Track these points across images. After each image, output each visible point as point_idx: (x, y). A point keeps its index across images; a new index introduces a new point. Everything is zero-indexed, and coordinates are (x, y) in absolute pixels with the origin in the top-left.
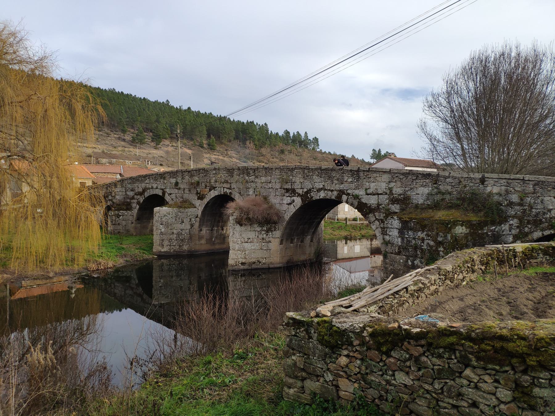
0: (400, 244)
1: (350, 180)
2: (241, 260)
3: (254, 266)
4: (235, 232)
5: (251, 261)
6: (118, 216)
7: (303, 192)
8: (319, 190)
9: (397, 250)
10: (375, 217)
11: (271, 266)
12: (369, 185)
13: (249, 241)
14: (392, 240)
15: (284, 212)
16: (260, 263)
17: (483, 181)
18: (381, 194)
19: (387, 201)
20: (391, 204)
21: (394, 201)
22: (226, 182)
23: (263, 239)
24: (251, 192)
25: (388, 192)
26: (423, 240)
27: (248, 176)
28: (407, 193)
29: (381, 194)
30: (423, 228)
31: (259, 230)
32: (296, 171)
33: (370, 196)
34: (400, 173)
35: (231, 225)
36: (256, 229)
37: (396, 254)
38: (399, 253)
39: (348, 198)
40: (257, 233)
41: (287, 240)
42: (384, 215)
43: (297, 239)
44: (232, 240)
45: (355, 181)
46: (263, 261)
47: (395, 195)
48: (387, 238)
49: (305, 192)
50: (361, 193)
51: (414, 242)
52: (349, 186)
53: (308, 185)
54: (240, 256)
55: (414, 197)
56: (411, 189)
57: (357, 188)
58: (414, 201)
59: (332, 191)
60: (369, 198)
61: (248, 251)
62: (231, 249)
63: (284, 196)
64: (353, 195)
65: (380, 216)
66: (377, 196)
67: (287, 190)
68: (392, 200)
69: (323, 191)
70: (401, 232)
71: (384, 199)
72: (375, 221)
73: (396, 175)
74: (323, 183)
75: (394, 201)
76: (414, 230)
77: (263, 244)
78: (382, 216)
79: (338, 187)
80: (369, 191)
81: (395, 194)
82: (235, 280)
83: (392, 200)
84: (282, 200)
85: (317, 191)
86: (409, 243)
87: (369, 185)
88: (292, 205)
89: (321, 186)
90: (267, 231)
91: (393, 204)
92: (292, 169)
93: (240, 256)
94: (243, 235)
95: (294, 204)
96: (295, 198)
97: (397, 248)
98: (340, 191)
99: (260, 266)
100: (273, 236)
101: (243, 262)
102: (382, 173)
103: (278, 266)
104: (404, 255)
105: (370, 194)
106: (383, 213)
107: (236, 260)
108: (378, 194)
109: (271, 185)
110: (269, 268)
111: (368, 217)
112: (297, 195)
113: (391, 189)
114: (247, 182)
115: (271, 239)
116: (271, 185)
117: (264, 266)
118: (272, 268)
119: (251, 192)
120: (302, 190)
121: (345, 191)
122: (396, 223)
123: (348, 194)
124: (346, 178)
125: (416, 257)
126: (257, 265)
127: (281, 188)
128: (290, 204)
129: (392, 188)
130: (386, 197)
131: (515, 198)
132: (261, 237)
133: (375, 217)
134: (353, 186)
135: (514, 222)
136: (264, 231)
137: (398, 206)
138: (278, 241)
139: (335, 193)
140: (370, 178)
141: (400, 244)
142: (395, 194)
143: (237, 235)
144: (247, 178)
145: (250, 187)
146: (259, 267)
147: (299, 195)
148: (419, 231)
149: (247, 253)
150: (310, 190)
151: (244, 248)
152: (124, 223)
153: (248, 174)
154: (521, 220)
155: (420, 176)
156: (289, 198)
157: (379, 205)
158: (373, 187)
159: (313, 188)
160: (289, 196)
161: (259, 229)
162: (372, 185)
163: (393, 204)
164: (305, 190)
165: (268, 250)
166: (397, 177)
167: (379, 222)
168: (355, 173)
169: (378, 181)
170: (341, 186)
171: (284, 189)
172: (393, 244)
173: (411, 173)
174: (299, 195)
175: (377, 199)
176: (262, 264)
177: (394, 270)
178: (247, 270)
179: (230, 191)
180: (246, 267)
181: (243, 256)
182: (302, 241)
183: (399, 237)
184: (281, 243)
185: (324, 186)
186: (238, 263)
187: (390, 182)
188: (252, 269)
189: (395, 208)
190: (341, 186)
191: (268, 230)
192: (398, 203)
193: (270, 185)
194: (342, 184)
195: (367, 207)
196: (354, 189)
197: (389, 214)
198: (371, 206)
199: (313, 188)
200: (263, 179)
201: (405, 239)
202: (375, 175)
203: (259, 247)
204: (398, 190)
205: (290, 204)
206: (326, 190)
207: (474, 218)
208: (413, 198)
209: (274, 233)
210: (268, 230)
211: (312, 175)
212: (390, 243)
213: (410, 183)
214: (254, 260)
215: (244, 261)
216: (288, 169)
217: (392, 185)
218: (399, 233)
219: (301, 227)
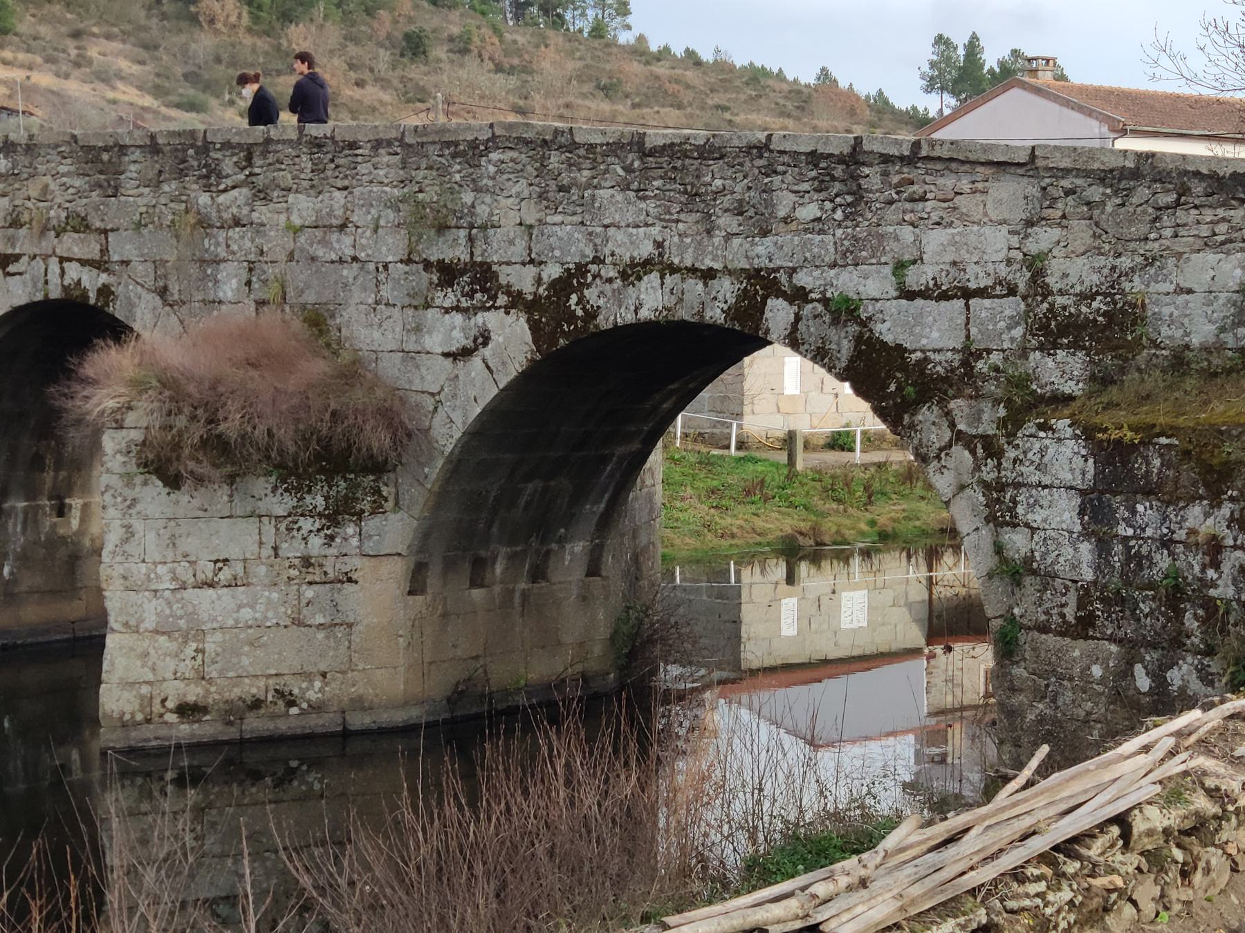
0: (1088, 575)
1: (809, 211)
2: (176, 692)
3: (255, 724)
4: (138, 525)
5: (237, 692)
7: (539, 281)
8: (633, 272)
9: (1070, 613)
10: (952, 425)
11: (359, 721)
12: (918, 240)
13: (225, 575)
14: (1043, 557)
15: (429, 403)
16: (292, 704)
18: (982, 293)
19: (1018, 332)
20: (1041, 348)
22: (80, 224)
23: (307, 562)
24: (229, 285)
25: (1022, 280)
27: (207, 188)
28: (1127, 286)
29: (982, 293)
31: (281, 512)
32: (494, 156)
33: (919, 302)
34: (1087, 174)
35: (115, 481)
36: (262, 507)
37: (1066, 631)
38: (1083, 627)
39: (798, 318)
40: (269, 529)
41: (449, 566)
42: (1002, 412)
43: (512, 557)
44: (119, 570)
45: (839, 215)
46: (312, 695)
47: (1060, 301)
48: (1017, 542)
49: (554, 284)
50: (872, 287)
51: (1163, 561)
52: (804, 245)
54: (171, 664)
55: (1166, 311)
56: (1150, 261)
57: (847, 258)
58: (1165, 331)
59: (708, 275)
60: (919, 317)
61: (218, 636)
62: (113, 622)
63: (427, 306)
64: (825, 301)
65: (976, 418)
66: (961, 302)
67: (448, 273)
68: (1045, 328)
69: (654, 277)
72: (949, 445)
73: (1066, 183)
74: (655, 231)
77: (309, 593)
78: (989, 420)
80: (917, 278)
81: (1061, 292)
82: (145, 806)
83: (1045, 328)
84: (418, 329)
85: (624, 275)
86: (1140, 566)
87: (918, 240)
88: (476, 361)
89: (646, 250)
90: (333, 517)
92: (474, 145)
93: (171, 664)
94: (189, 544)
95: (487, 352)
96: (492, 319)
97: (1072, 598)
98: (754, 275)
99: (293, 722)
100: (369, 547)
101: (191, 698)
102: (988, 171)
103: (400, 717)
104: (1112, 639)
105: (924, 294)
106: (997, 402)
107: (145, 690)
108: (967, 294)
109: (348, 240)
110: (346, 735)
111: (912, 426)
112: (502, 300)
113: (1036, 266)
114: (203, 223)
115: (357, 562)
116: (348, 240)
117: (316, 723)
118: (364, 733)
119: (229, 285)
120: (531, 270)
121: (783, 278)
123: (799, 296)
124: (784, 202)
126: (274, 717)
127: (408, 261)
128: (464, 354)
129: (1042, 256)
130: (1012, 306)
132: (293, 549)
133: (952, 425)
134: (825, 245)
136: (312, 513)
137: (1076, 363)
138: (395, 572)
139: (727, 289)
140: (923, 199)
141: (1088, 575)
142: (1061, 292)
143: (149, 540)
144: (204, 199)
145: (222, 252)
146: (283, 726)
147: (517, 301)
148: (1193, 499)
149: (210, 647)
150: (581, 269)
151: (192, 616)
153: (211, 177)
155: (1198, 188)
156: (458, 318)
157: (970, 355)
159: (597, 260)
160: (457, 309)
161: (281, 504)
162: (935, 239)
163: (1048, 347)
164: (553, 271)
165: (339, 625)
166: (1068, 192)
167: (973, 452)
168: (839, 171)
169: (966, 220)
170: (760, 250)
171: (428, 265)
172: (1047, 578)
173: (1146, 169)
174: (517, 301)
175: (961, 320)
176: (303, 712)
177: (1055, 722)
178: (213, 746)
179: (104, 278)
180: (205, 729)
181: (187, 668)
182: (538, 574)
183: (1086, 534)
184: (416, 586)
185: (659, 245)
186: (157, 708)
187: (1030, 223)
188: (242, 743)
190: (760, 250)
191: (337, 512)
192: (1075, 346)
193: (344, 244)
194: (765, 233)
195: (905, 367)
196: (833, 265)
198: (926, 360)
199: (597, 260)
200: (303, 207)
201: (1118, 548)
202: (948, 182)
203: (282, 613)
205: (464, 354)
206: (674, 270)
208: (1158, 316)
209: (371, 524)
210: (337, 512)
211: (589, 185)
212: (1034, 573)
213: (1143, 229)
214: (254, 689)
215: (193, 694)
216: (448, 144)
217: (1043, 238)
218: (1081, 513)
219: (530, 487)
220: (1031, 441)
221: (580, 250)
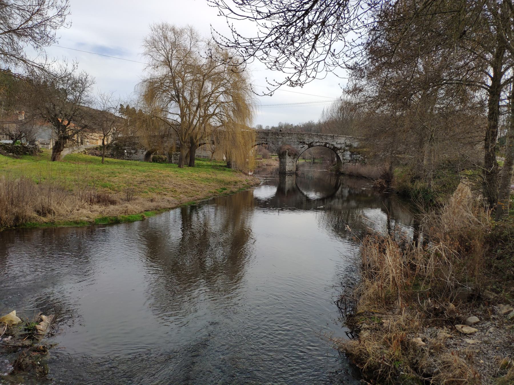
8: (316, 142)
21: (347, 146)
26: (359, 157)
30: (359, 154)
38: (350, 162)
48: (344, 158)
53: (311, 140)
67: (301, 142)
70: (351, 156)
71: (343, 146)
75: (347, 146)
76: (356, 155)
78: (342, 151)
79: (325, 141)
91: (346, 147)
113: (346, 142)
122: (349, 153)
139: (324, 144)
147: (307, 144)
153: (278, 135)
157: (341, 147)
158: (339, 141)
162: (339, 141)
174: (307, 144)
189: (347, 148)
197: (345, 150)
200: (287, 137)
204: (348, 143)
217: (346, 141)
220: (346, 152)
221: (312, 141)
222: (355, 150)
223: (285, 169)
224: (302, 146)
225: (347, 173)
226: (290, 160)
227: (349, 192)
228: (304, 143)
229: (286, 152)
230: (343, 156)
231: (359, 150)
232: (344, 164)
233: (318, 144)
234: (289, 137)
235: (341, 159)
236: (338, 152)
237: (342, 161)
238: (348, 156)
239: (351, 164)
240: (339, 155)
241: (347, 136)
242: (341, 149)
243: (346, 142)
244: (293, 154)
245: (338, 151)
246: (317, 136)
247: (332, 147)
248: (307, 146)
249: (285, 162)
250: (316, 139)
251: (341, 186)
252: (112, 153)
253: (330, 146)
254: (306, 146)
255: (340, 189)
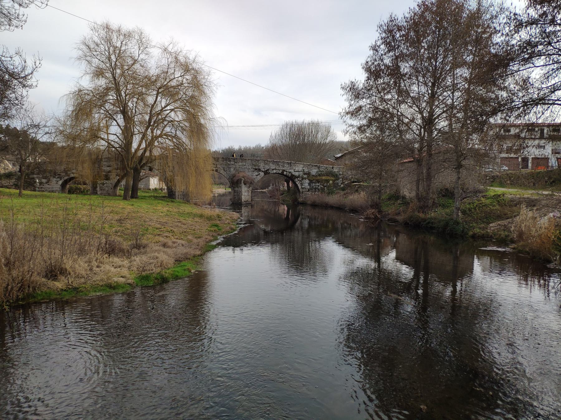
6: (103, 184)
8: (273, 170)
17: (333, 168)
21: (305, 174)
24: (232, 170)
26: (319, 186)
38: (309, 191)
48: (303, 187)
53: (267, 167)
67: (256, 169)
70: (309, 184)
71: (301, 173)
76: (315, 183)
78: (301, 179)
79: (282, 169)
113: (304, 170)
114: (229, 164)
119: (232, 170)
122: (307, 181)
123: (287, 171)
125: (315, 191)
131: (341, 173)
134: (289, 168)
135: (341, 179)
139: (281, 171)
152: (107, 189)
153: (230, 161)
154: (343, 179)
157: (299, 175)
158: (297, 169)
162: (297, 168)
189: (305, 176)
197: (303, 179)
200: (240, 164)
204: (306, 170)
207: (333, 179)
217: (304, 168)
220: (304, 181)
222: (314, 178)
223: (240, 199)
224: (257, 173)
225: (309, 202)
226: (246, 189)
227: (309, 223)
228: (259, 170)
229: (241, 180)
230: (302, 184)
231: (318, 178)
232: (302, 193)
233: (275, 171)
234: (243, 163)
235: (300, 187)
236: (296, 180)
237: (301, 190)
238: (307, 184)
239: (310, 193)
240: (297, 183)
241: (305, 163)
242: (299, 177)
243: (304, 170)
244: (248, 182)
245: (296, 179)
246: (274, 162)
247: (290, 175)
248: (263, 173)
249: (241, 192)
250: (273, 166)
251: (301, 217)
252: (16, 183)
253: (288, 174)
254: (262, 174)
255: (299, 219)
